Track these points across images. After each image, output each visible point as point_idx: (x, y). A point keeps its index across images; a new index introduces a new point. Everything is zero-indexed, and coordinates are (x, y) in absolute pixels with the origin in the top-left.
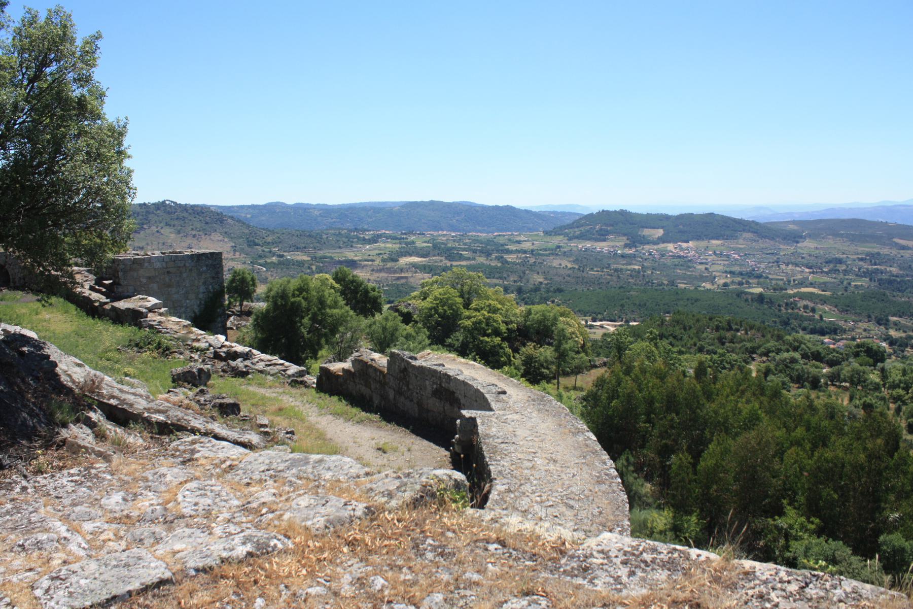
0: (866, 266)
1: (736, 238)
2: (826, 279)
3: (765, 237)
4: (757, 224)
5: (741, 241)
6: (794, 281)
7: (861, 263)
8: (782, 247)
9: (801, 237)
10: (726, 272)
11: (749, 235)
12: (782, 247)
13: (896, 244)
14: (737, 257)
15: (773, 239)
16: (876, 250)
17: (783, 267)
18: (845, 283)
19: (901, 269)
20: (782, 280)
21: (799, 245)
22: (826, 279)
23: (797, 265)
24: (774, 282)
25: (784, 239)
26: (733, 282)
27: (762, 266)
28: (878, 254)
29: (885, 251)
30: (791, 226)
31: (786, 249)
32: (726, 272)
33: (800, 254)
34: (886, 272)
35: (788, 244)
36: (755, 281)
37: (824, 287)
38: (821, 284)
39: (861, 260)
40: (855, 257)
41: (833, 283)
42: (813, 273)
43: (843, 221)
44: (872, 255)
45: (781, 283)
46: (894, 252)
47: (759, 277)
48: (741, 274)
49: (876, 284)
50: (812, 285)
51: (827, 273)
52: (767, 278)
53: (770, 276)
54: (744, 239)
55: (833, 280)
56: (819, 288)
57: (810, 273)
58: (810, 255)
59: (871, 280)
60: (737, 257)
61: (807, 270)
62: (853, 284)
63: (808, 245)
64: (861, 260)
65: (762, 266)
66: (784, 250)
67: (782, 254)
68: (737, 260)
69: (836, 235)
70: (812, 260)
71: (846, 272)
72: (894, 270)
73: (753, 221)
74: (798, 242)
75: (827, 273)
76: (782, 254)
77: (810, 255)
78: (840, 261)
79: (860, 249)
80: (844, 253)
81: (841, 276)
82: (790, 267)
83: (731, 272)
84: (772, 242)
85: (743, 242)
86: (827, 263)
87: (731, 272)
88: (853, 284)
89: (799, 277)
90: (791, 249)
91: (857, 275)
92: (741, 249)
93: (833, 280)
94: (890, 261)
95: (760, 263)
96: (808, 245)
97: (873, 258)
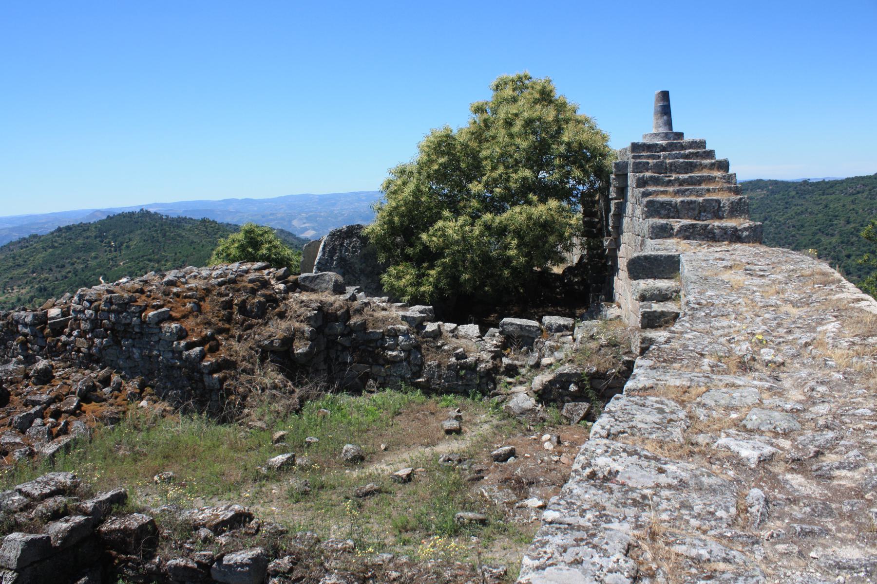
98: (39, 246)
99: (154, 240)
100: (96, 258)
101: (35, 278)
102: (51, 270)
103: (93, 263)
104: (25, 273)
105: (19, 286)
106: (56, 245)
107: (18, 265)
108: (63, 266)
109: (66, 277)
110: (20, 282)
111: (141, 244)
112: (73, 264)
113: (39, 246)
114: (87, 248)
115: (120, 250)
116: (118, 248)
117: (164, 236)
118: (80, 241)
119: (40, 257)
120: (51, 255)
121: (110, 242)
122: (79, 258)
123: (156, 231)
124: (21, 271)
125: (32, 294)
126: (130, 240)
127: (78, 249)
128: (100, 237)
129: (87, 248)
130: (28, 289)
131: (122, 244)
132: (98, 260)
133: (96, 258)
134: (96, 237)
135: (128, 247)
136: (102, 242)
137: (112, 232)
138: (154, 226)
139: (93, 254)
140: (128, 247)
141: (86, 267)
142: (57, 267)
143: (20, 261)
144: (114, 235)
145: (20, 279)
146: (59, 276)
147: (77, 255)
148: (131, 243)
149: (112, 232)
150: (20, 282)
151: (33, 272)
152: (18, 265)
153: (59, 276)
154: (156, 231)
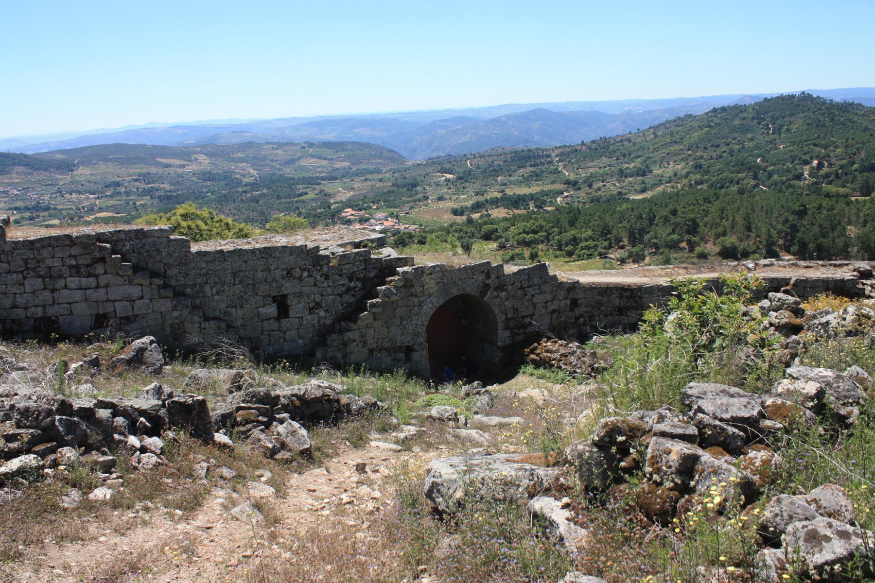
0: (142, 186)
1: (8, 173)
2: (112, 202)
3: (39, 169)
4: (26, 156)
5: (14, 175)
6: (83, 208)
7: (137, 184)
8: (58, 177)
9: (74, 165)
10: (10, 209)
11: (21, 169)
12: (58, 177)
13: (160, 163)
14: (15, 192)
15: (47, 170)
16: (145, 171)
17: (67, 196)
18: (131, 203)
19: (171, 185)
20: (71, 209)
21: (74, 173)
22: (112, 202)
23: (80, 193)
24: (63, 212)
25: (58, 169)
26: (23, 218)
27: (47, 197)
28: (149, 173)
29: (153, 170)
30: (59, 156)
31: (63, 179)
32: (10, 209)
33: (78, 181)
34: (161, 189)
35: (64, 174)
36: (45, 213)
37: (115, 209)
38: (112, 206)
39: (136, 180)
40: (130, 178)
41: (120, 205)
42: (98, 198)
43: (106, 146)
44: (144, 175)
45: (71, 212)
46: (160, 170)
47: (47, 209)
48: (27, 209)
49: (157, 200)
50: (101, 210)
51: (112, 196)
52: (55, 209)
53: (58, 207)
54: (17, 173)
55: (119, 203)
56: (111, 211)
57: (96, 198)
58: (89, 182)
59: (151, 197)
60: (15, 192)
61: (92, 196)
62: (138, 203)
63: (83, 172)
64: (136, 180)
65: (47, 197)
66: (61, 179)
67: (61, 183)
68: (16, 195)
69: (106, 160)
70: (92, 186)
71: (127, 193)
72: (167, 186)
73: (21, 154)
74: (72, 171)
75: (112, 196)
76: (61, 183)
77: (89, 182)
78: (118, 184)
79: (131, 171)
80: (118, 176)
81: (124, 197)
82: (74, 195)
83: (16, 209)
84: (47, 173)
85: (16, 176)
86: (106, 187)
87: (16, 209)
88: (138, 203)
89: (86, 204)
90: (68, 178)
91: (138, 195)
92: (17, 183)
93: (119, 203)
94: (161, 179)
95: (42, 195)
96: (83, 172)
97: (145, 177)
98: (695, 124)
99: (819, 125)
100: (752, 140)
101: (690, 155)
102: (706, 148)
103: (748, 144)
104: (681, 150)
105: (675, 161)
106: (712, 124)
107: (675, 142)
108: (718, 146)
109: (721, 157)
110: (675, 158)
111: (804, 128)
112: (728, 144)
113: (695, 124)
114: (744, 129)
115: (780, 133)
116: (778, 131)
117: (832, 120)
118: (737, 122)
119: (696, 135)
120: (707, 133)
121: (768, 125)
122: (734, 139)
123: (823, 114)
124: (677, 147)
125: (687, 170)
126: (791, 123)
127: (734, 130)
128: (758, 118)
129: (744, 129)
130: (683, 165)
131: (782, 126)
132: (755, 142)
133: (752, 140)
134: (753, 119)
135: (788, 130)
136: (760, 124)
137: (770, 114)
138: (820, 109)
139: (749, 136)
140: (788, 130)
141: (743, 148)
142: (712, 146)
143: (677, 138)
144: (772, 117)
145: (676, 155)
146: (714, 155)
147: (732, 135)
148: (792, 126)
149: (770, 114)
150: (675, 158)
151: (689, 150)
152: (675, 142)
153: (714, 155)
154: (823, 114)
